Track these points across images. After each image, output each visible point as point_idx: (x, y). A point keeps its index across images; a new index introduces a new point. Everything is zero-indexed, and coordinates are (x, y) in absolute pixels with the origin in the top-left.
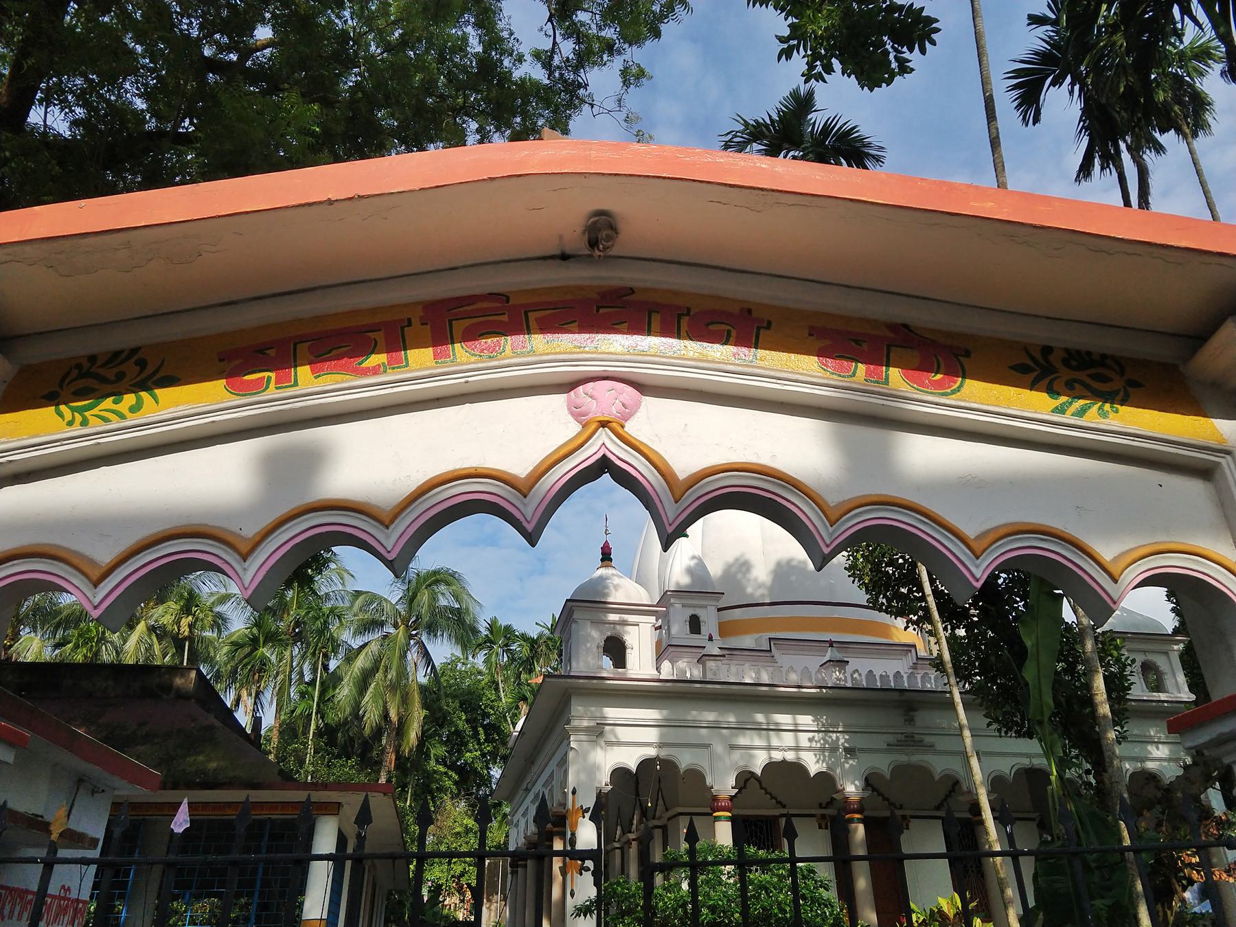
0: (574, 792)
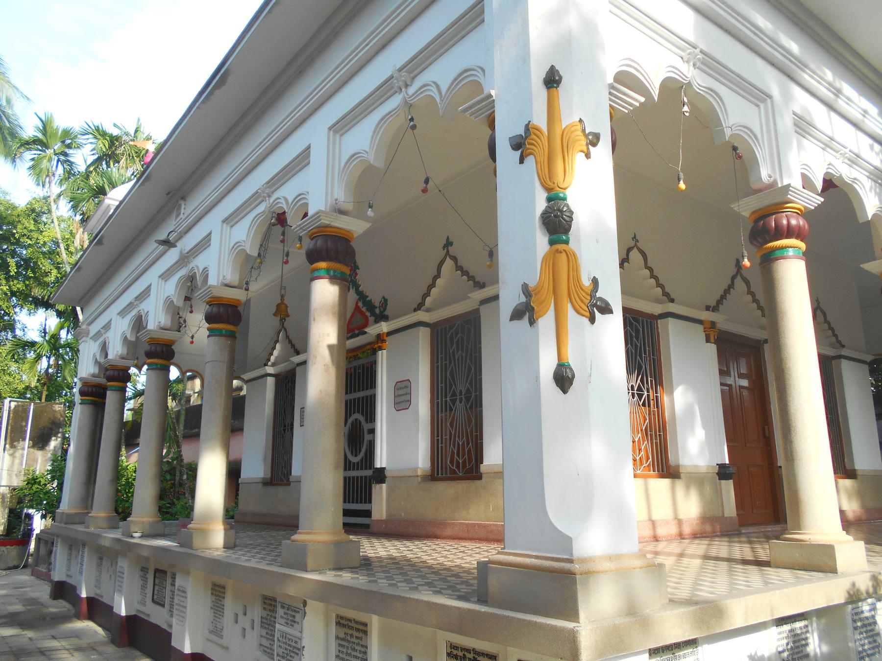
0: (552, 80)
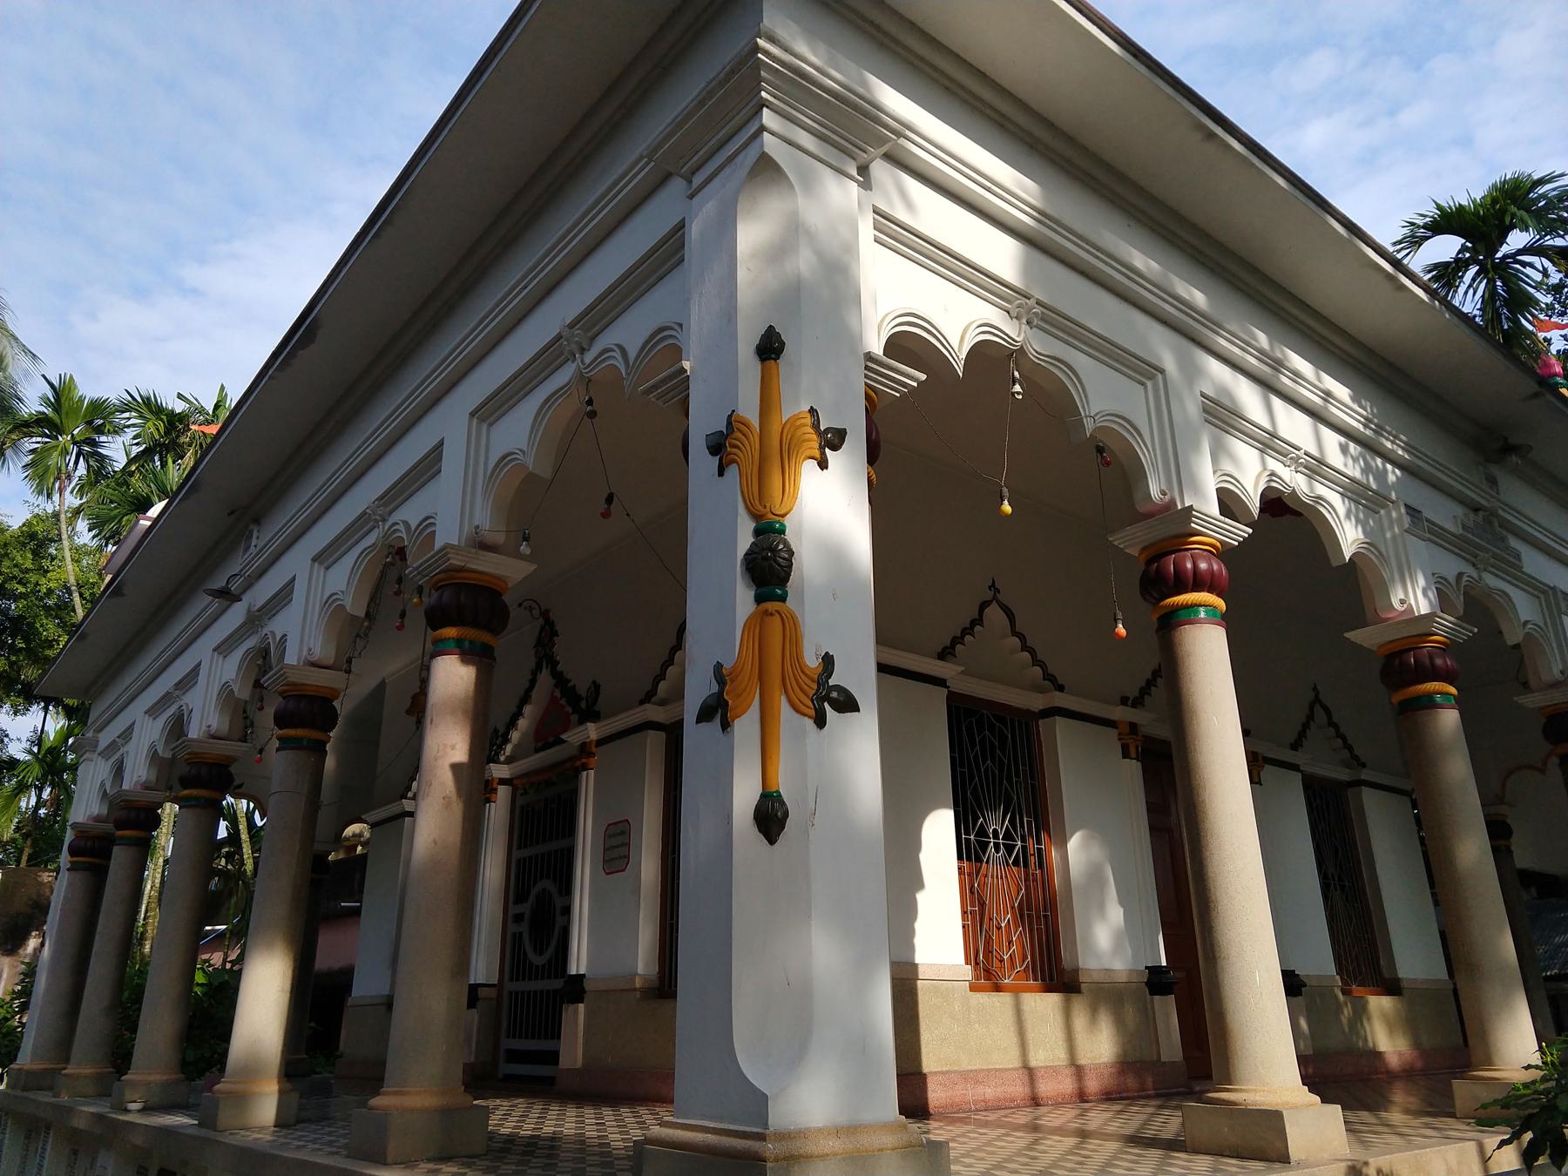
0: (770, 348)
